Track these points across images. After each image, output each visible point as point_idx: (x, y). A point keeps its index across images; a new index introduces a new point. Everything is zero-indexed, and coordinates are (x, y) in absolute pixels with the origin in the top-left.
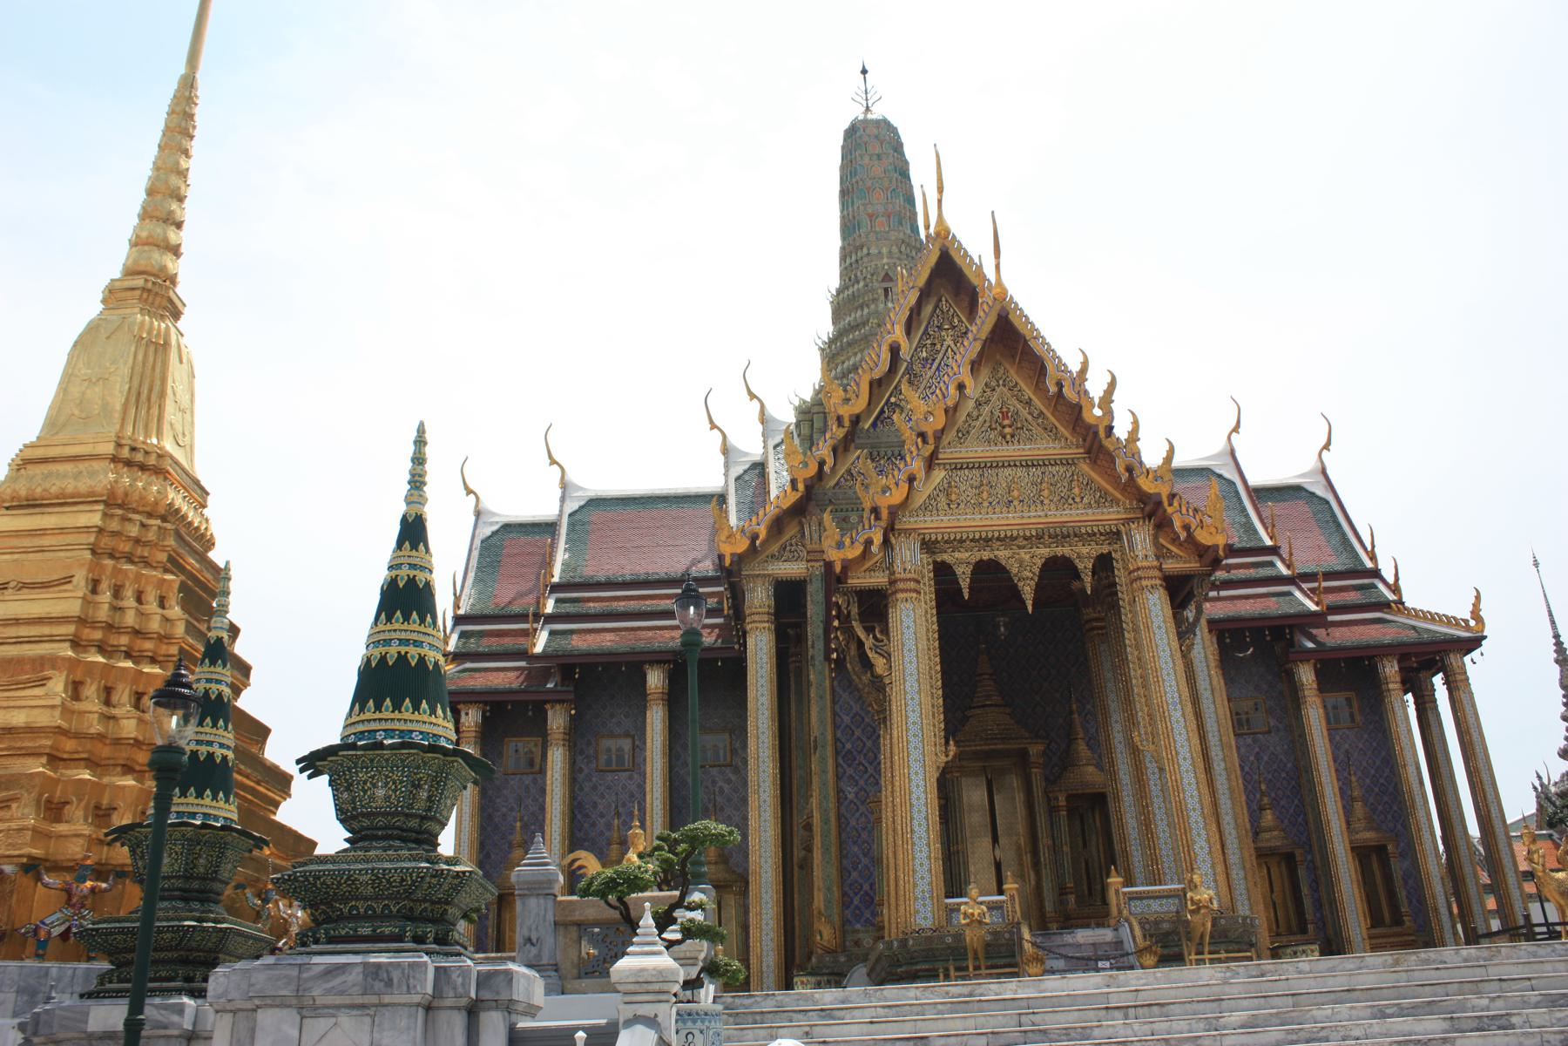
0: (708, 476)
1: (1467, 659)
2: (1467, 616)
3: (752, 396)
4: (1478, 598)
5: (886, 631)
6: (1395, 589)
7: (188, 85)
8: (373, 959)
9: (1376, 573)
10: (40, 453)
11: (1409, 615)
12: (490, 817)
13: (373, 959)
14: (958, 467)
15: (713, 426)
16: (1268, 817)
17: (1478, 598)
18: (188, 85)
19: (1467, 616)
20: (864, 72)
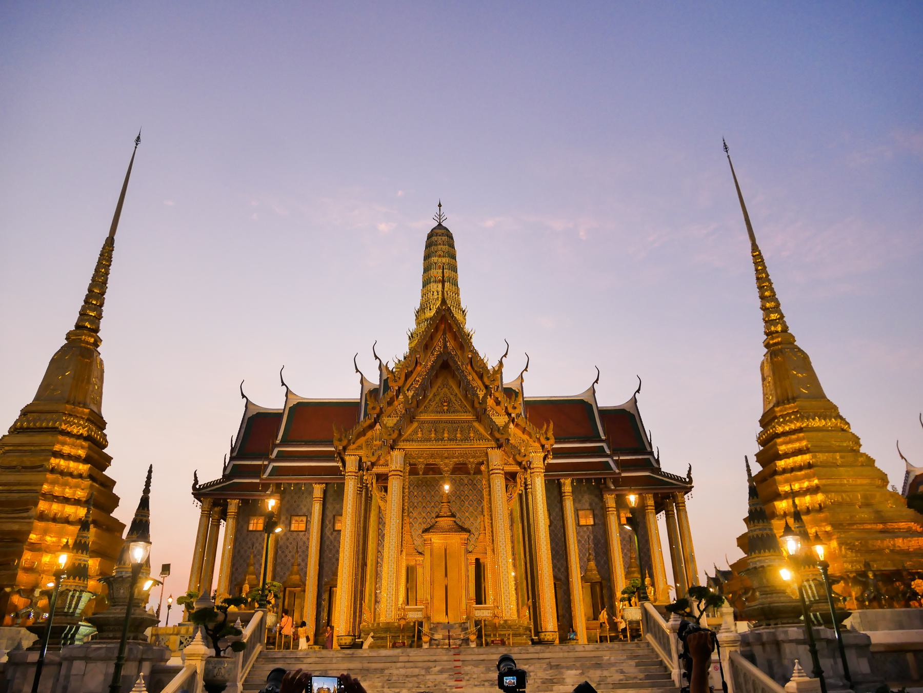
0: (352, 393)
1: (686, 496)
2: (685, 476)
3: (376, 357)
4: (690, 468)
5: (386, 491)
6: (658, 461)
7: (110, 243)
8: (109, 646)
9: (652, 453)
10: (34, 409)
11: (661, 475)
12: (239, 551)
13: (109, 646)
14: (423, 422)
15: (357, 371)
16: (592, 564)
17: (690, 468)
18: (110, 243)
19: (685, 476)
20: (440, 205)
